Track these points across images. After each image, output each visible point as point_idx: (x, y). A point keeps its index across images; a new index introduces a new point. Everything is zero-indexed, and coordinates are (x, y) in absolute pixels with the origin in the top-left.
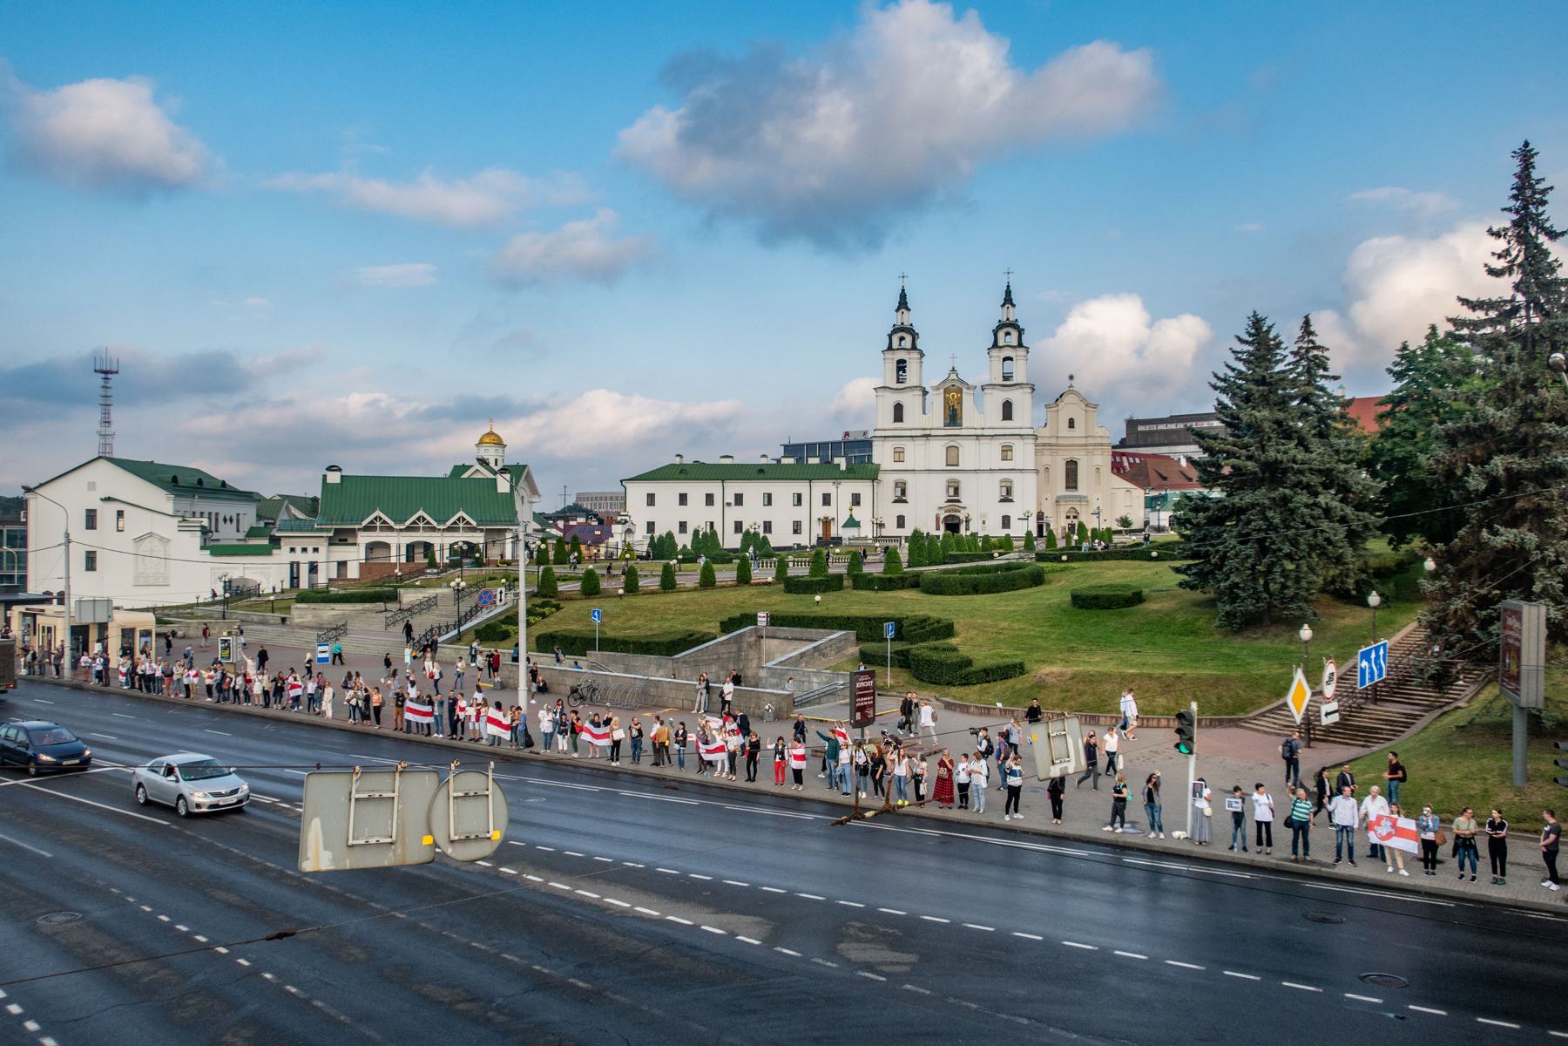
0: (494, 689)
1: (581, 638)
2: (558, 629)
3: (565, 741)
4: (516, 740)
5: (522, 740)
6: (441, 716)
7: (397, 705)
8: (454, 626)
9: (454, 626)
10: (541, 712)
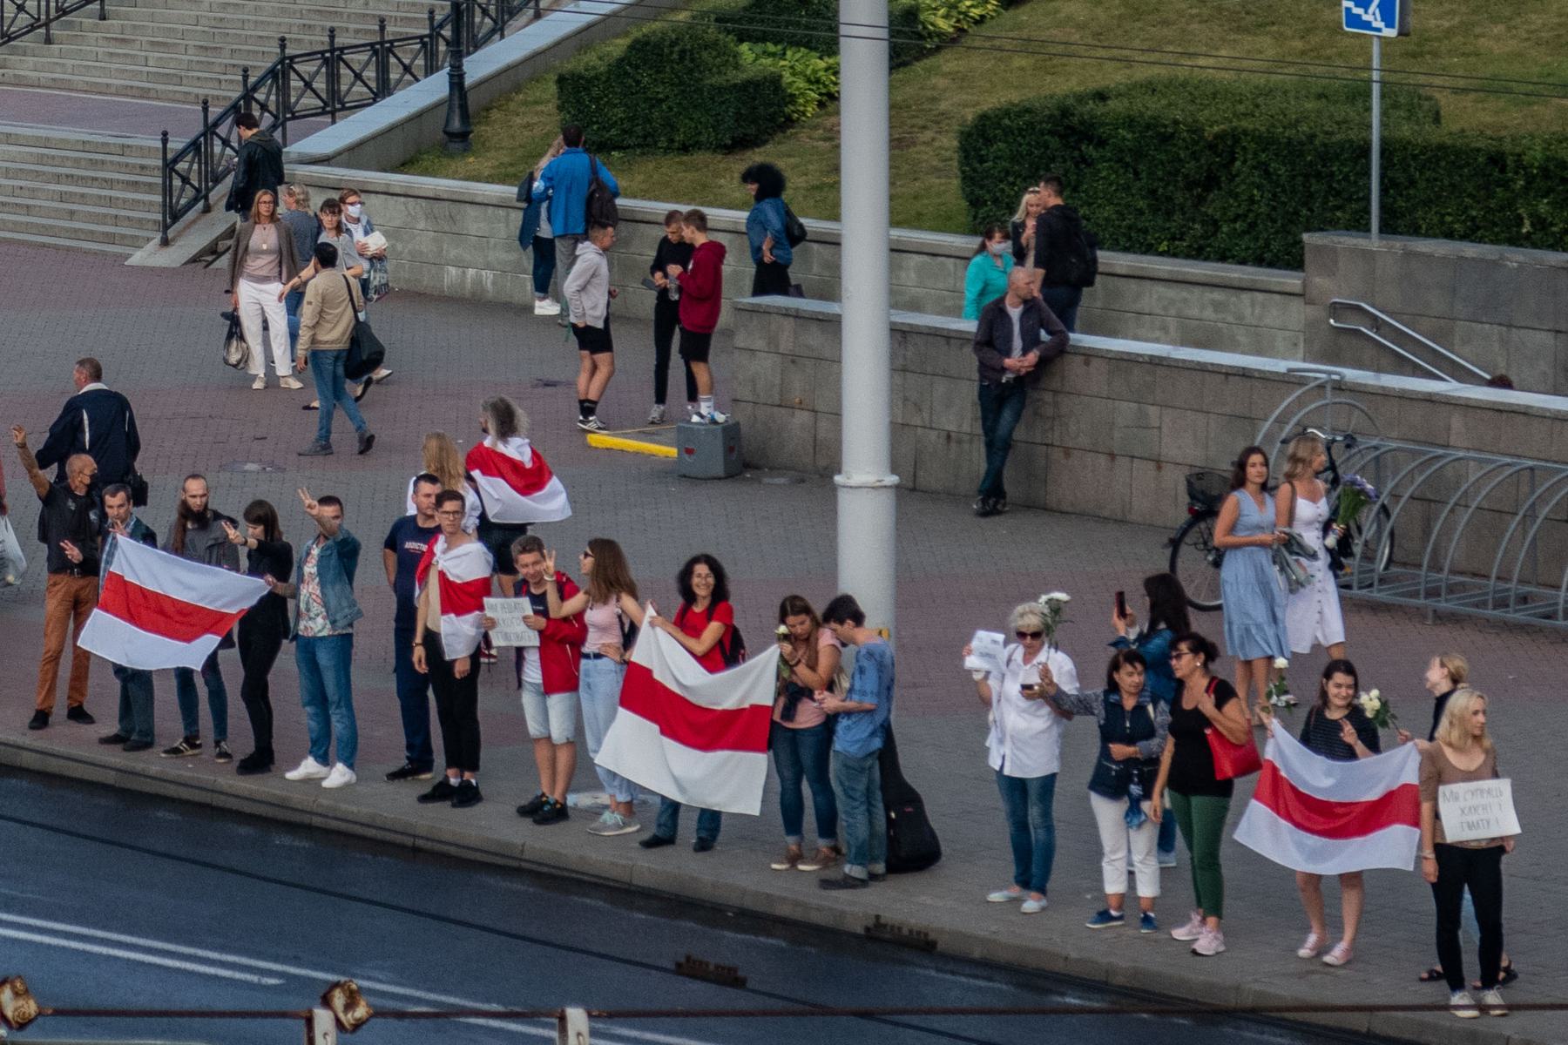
0: (681, 475)
1: (1265, 142)
2: (1114, 77)
3: (1144, 840)
4: (828, 826)
5: (855, 823)
6: (344, 643)
7: (59, 564)
8: (428, 44)
9: (428, 44)
10: (984, 639)
